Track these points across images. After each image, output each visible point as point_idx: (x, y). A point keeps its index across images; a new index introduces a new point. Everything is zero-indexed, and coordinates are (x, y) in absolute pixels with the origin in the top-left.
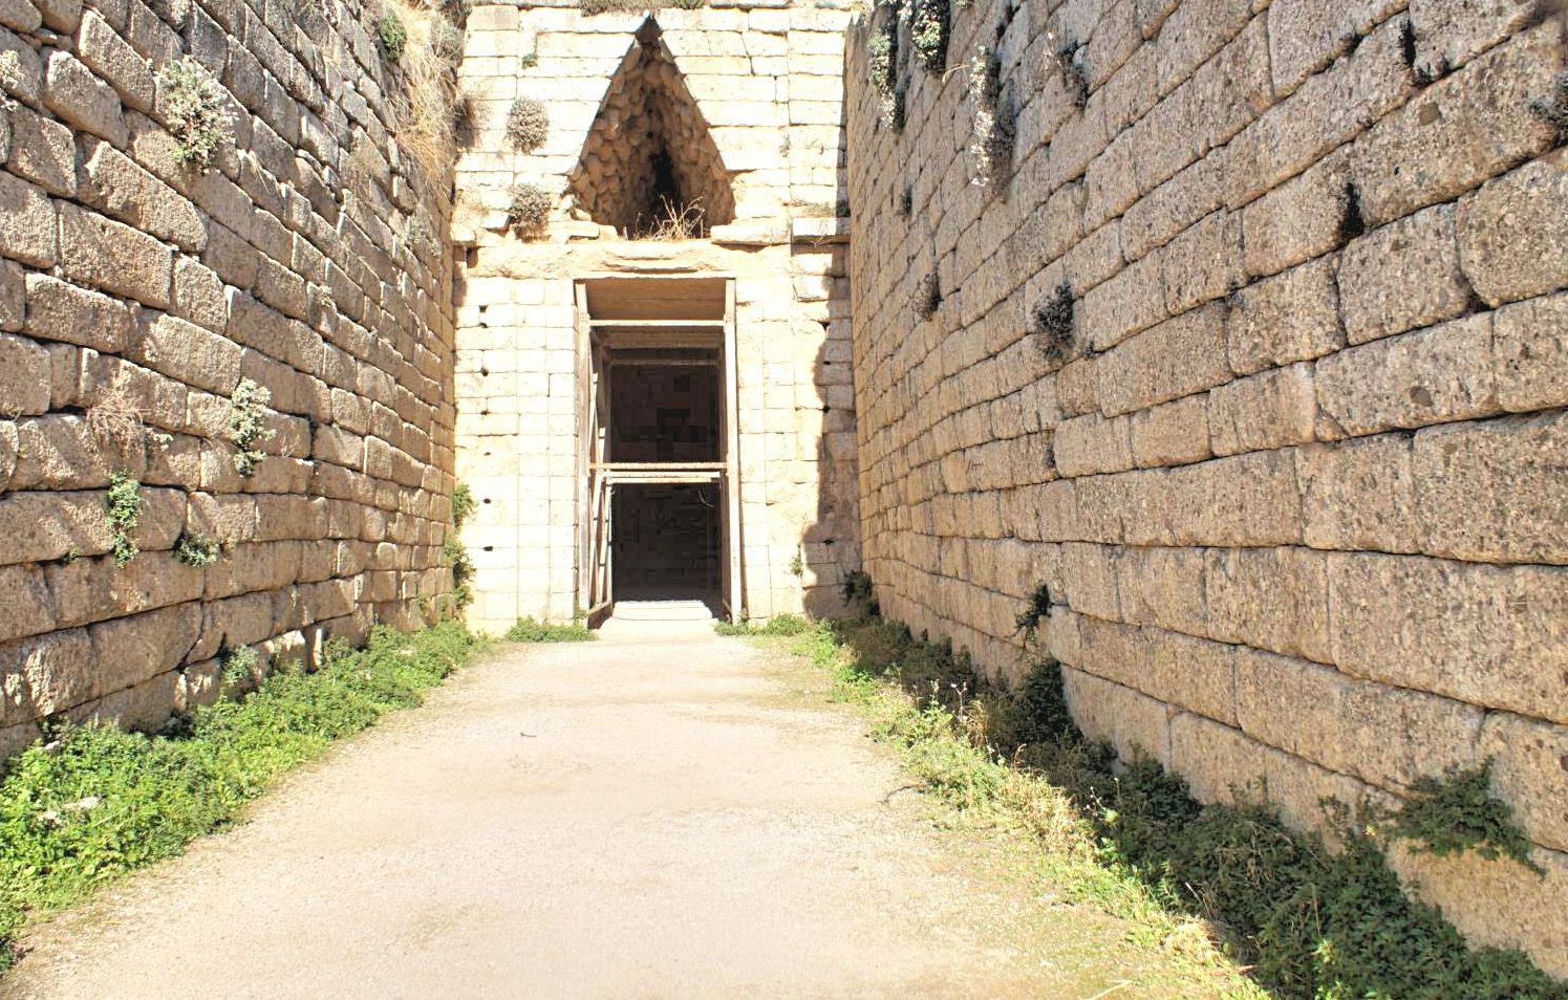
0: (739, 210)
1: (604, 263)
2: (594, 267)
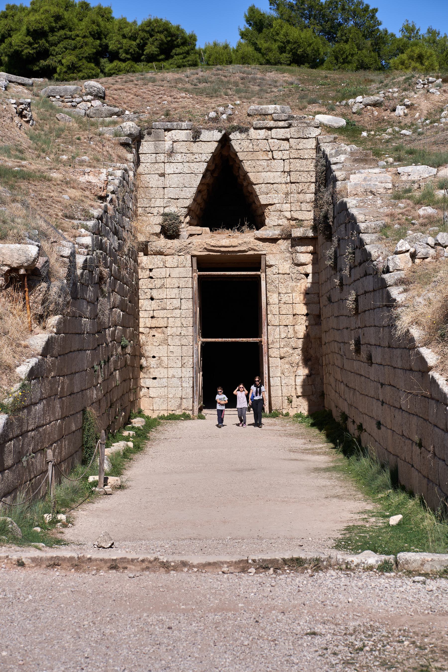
0: (267, 221)
1: (205, 248)
2: (201, 250)
